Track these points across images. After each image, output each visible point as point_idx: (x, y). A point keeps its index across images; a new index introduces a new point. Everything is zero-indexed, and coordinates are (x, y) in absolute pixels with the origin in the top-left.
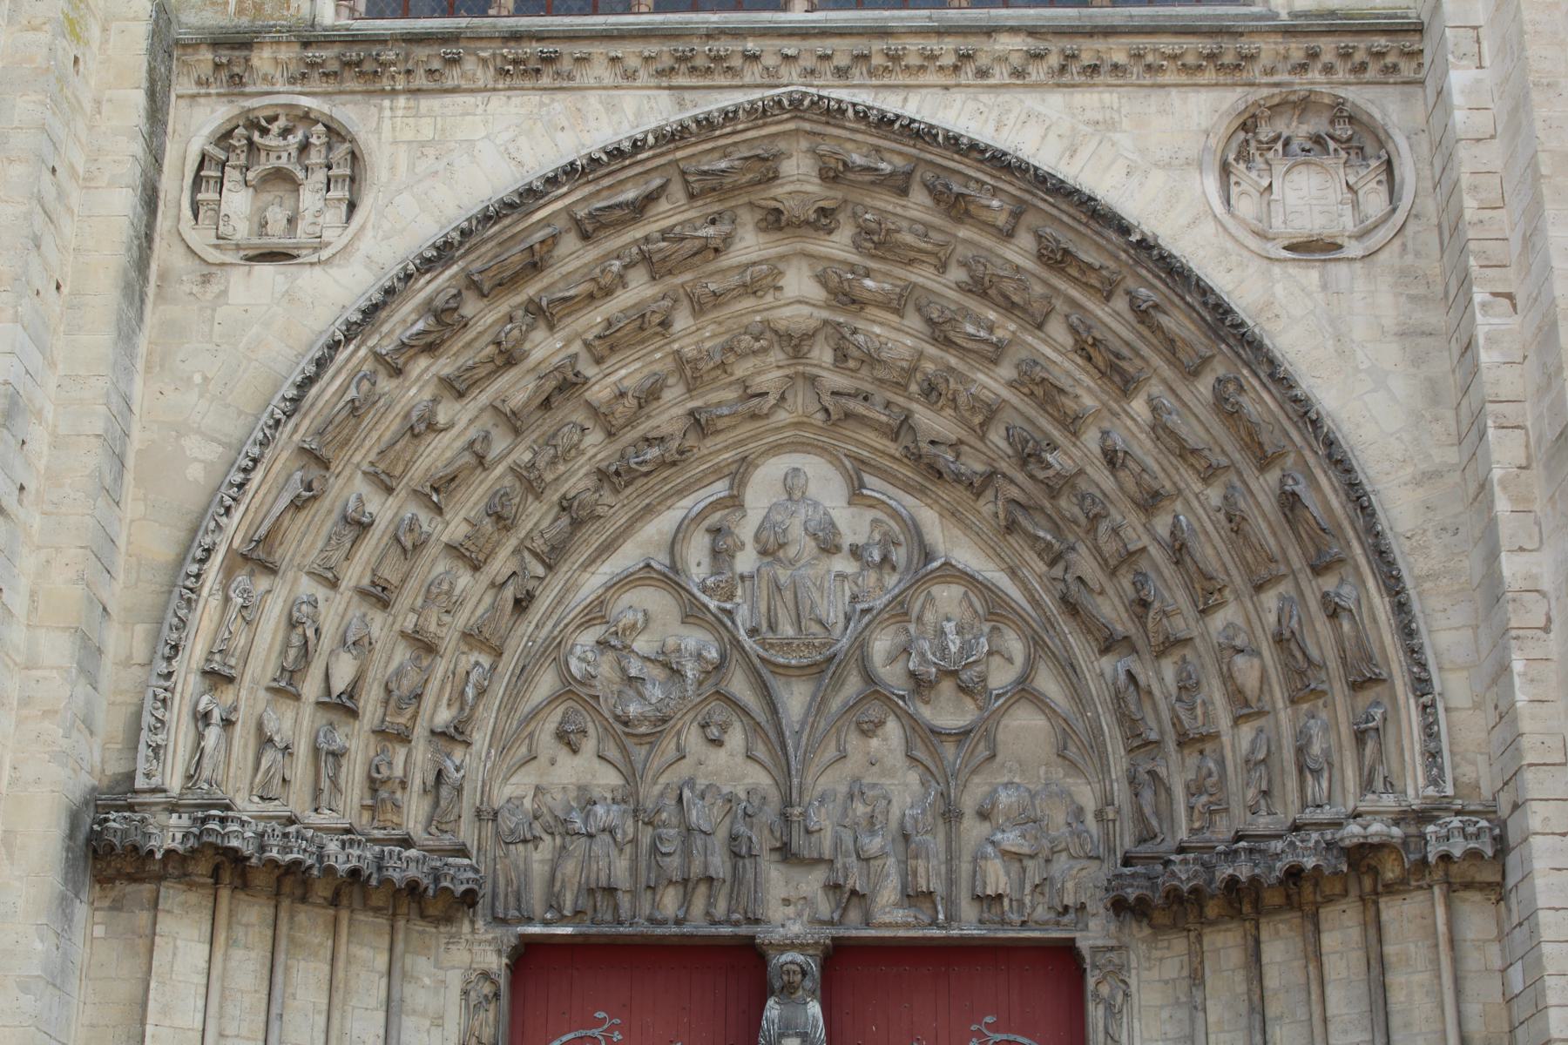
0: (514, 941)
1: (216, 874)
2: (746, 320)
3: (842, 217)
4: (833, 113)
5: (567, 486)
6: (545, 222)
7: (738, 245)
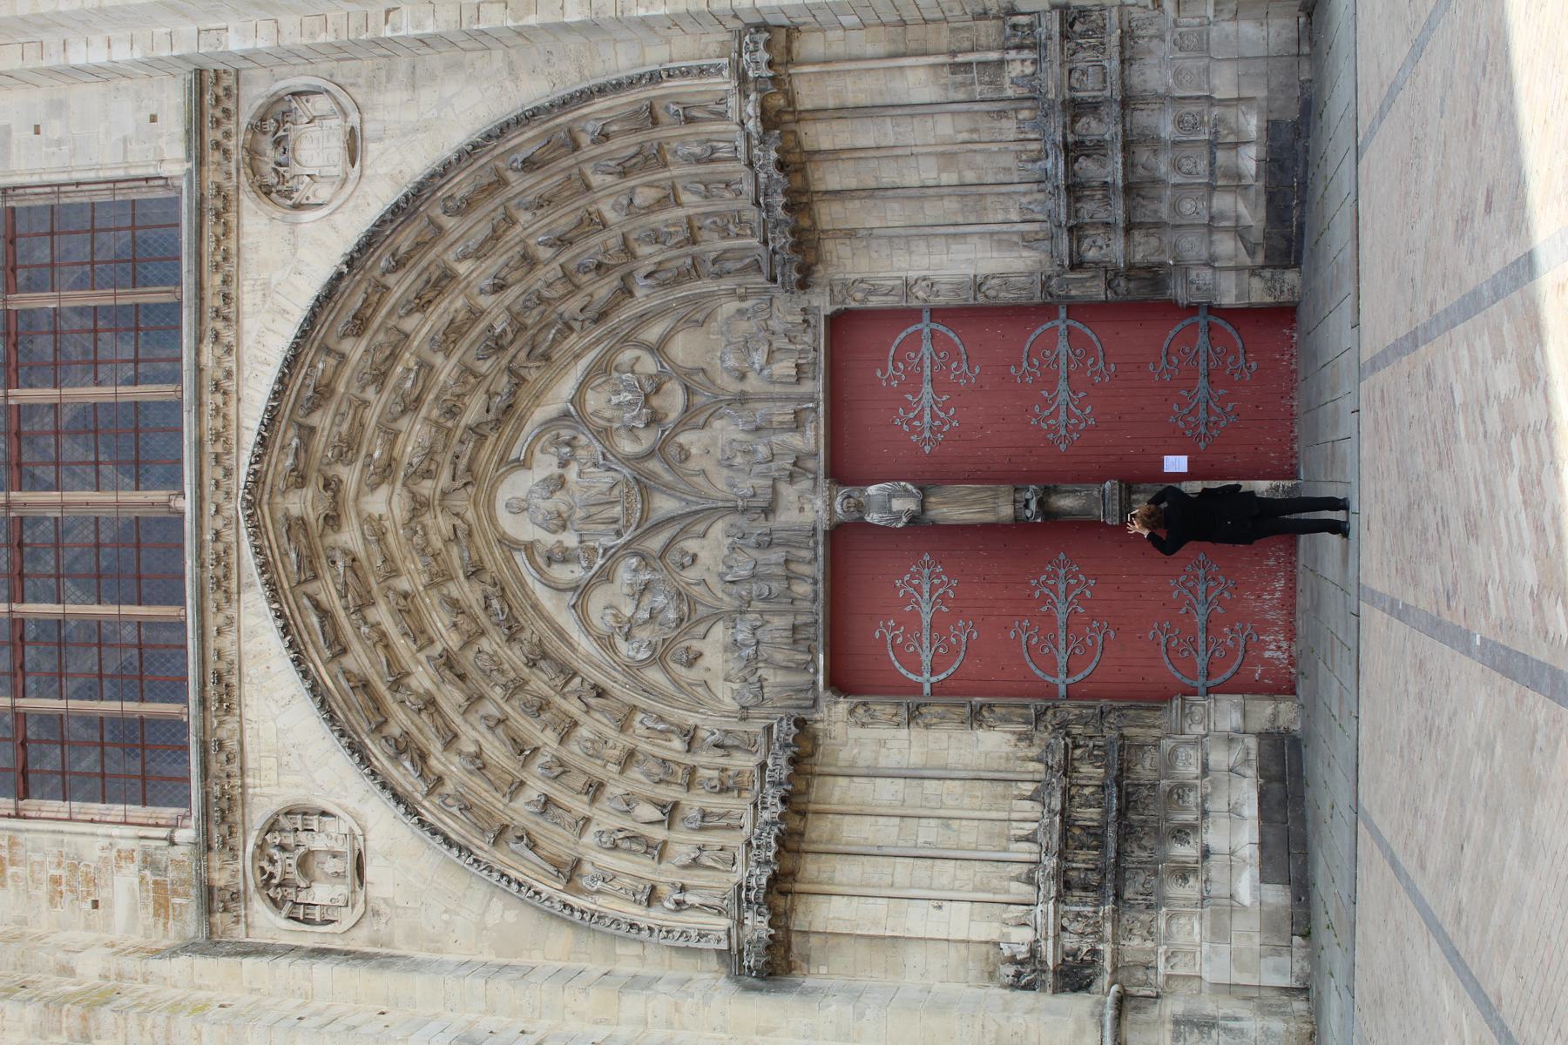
0: (829, 693)
1: (784, 893)
2: (403, 540)
3: (330, 473)
4: (257, 478)
5: (519, 663)
6: (334, 678)
7: (350, 545)
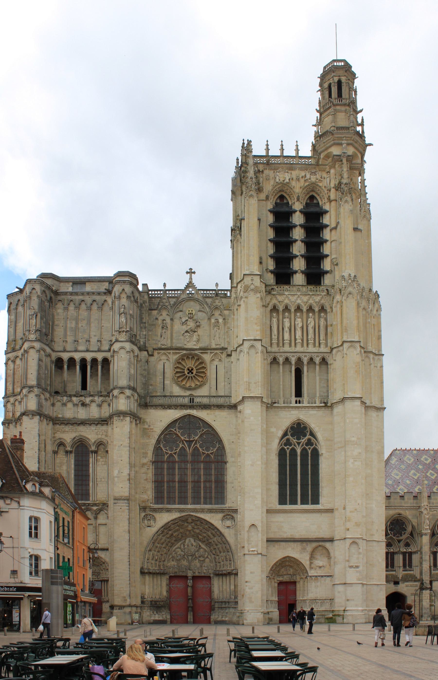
4: (192, 516)
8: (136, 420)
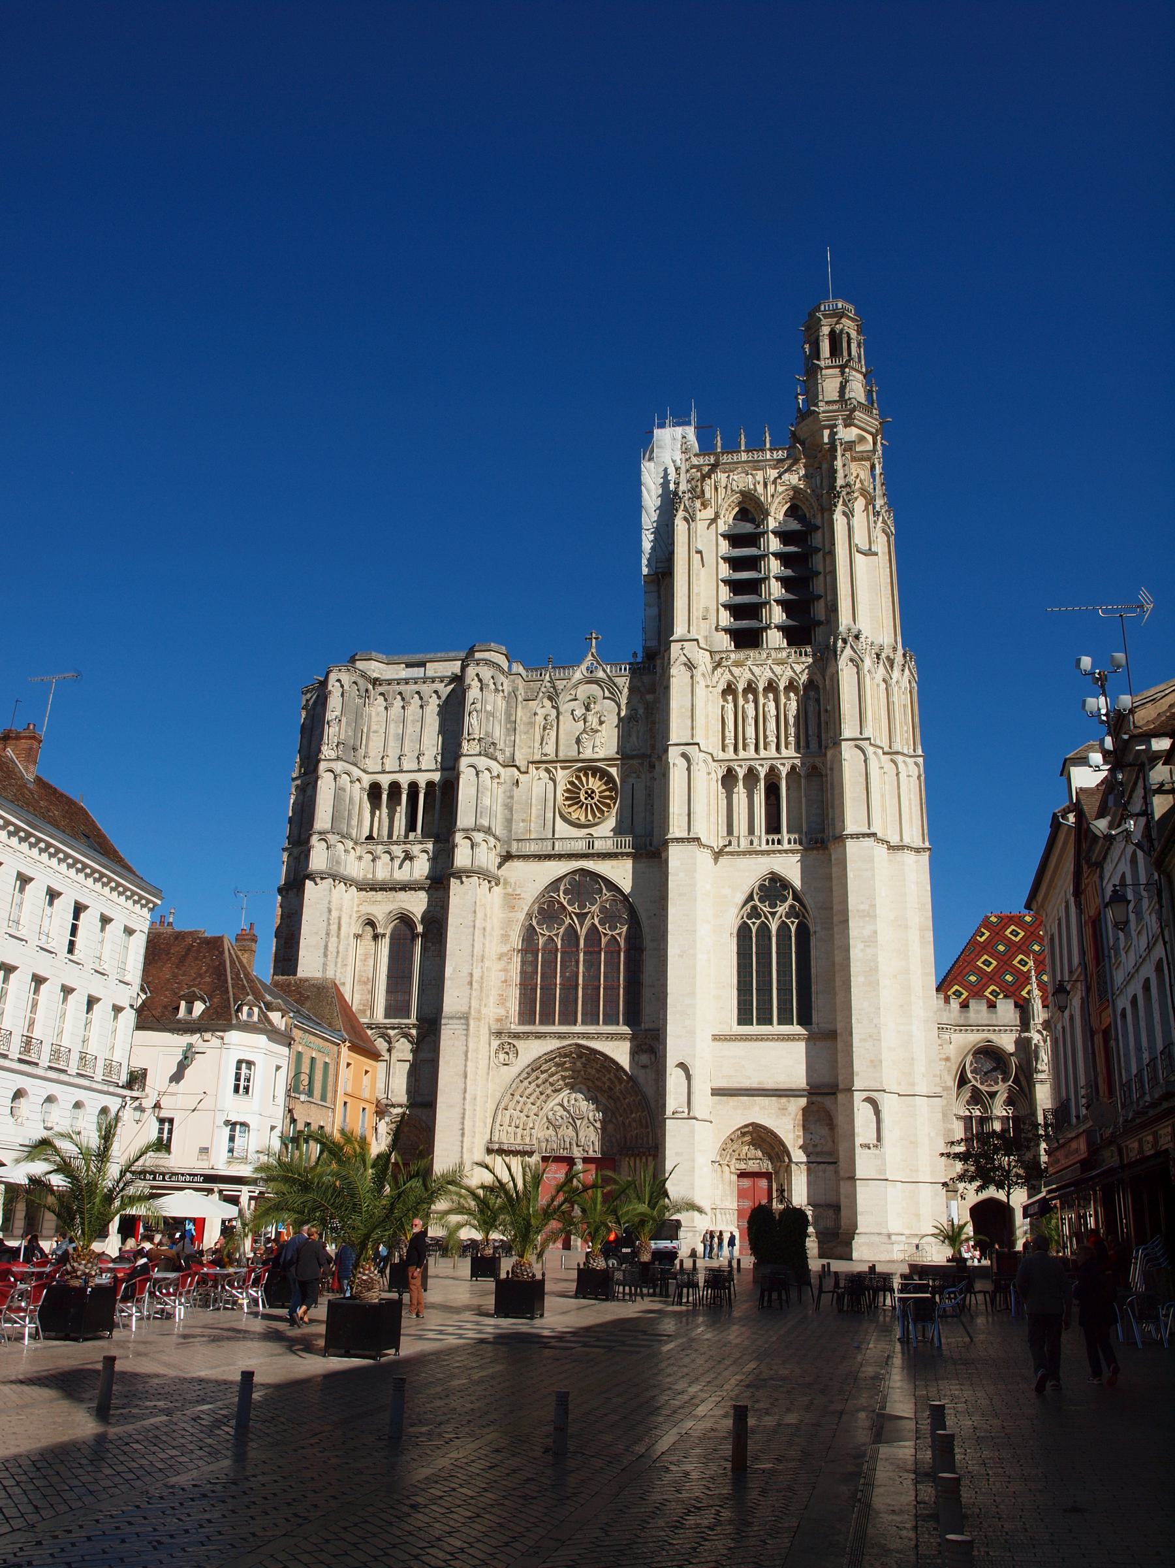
8: (489, 882)
